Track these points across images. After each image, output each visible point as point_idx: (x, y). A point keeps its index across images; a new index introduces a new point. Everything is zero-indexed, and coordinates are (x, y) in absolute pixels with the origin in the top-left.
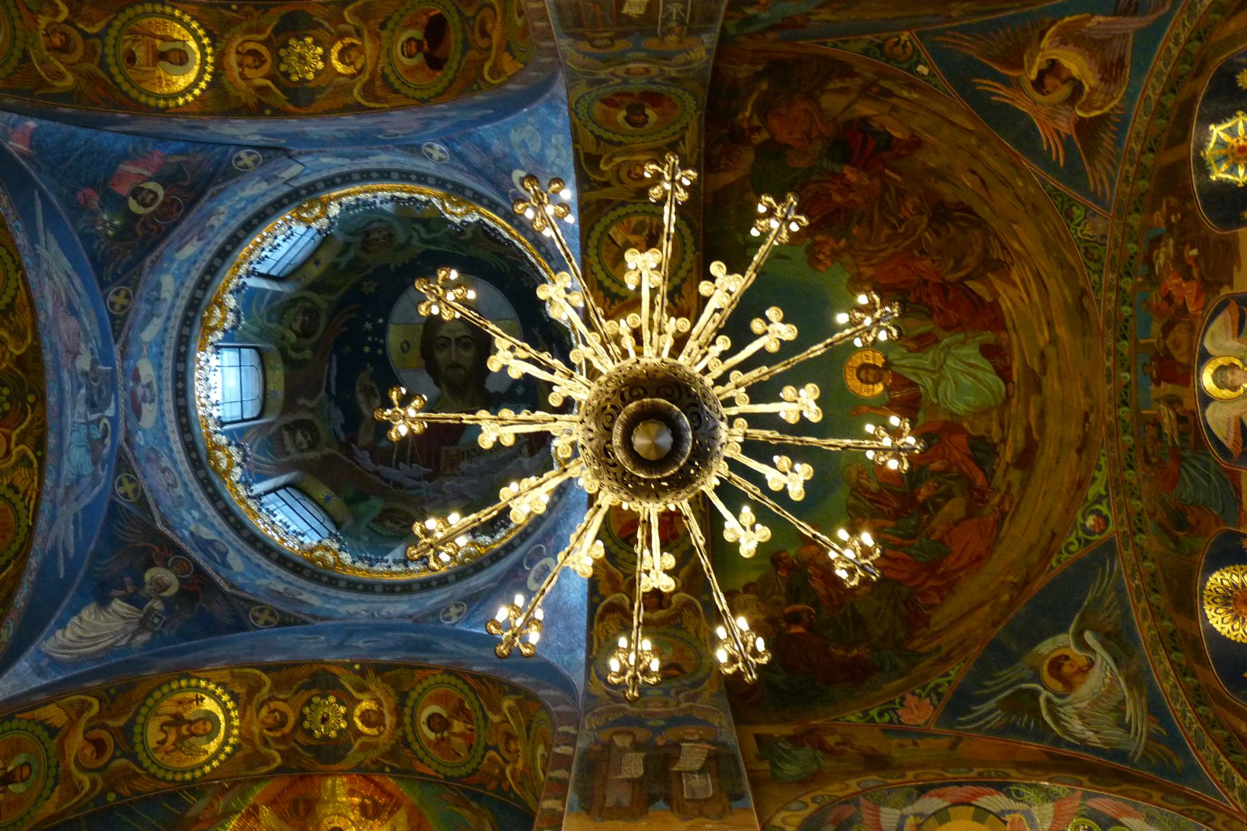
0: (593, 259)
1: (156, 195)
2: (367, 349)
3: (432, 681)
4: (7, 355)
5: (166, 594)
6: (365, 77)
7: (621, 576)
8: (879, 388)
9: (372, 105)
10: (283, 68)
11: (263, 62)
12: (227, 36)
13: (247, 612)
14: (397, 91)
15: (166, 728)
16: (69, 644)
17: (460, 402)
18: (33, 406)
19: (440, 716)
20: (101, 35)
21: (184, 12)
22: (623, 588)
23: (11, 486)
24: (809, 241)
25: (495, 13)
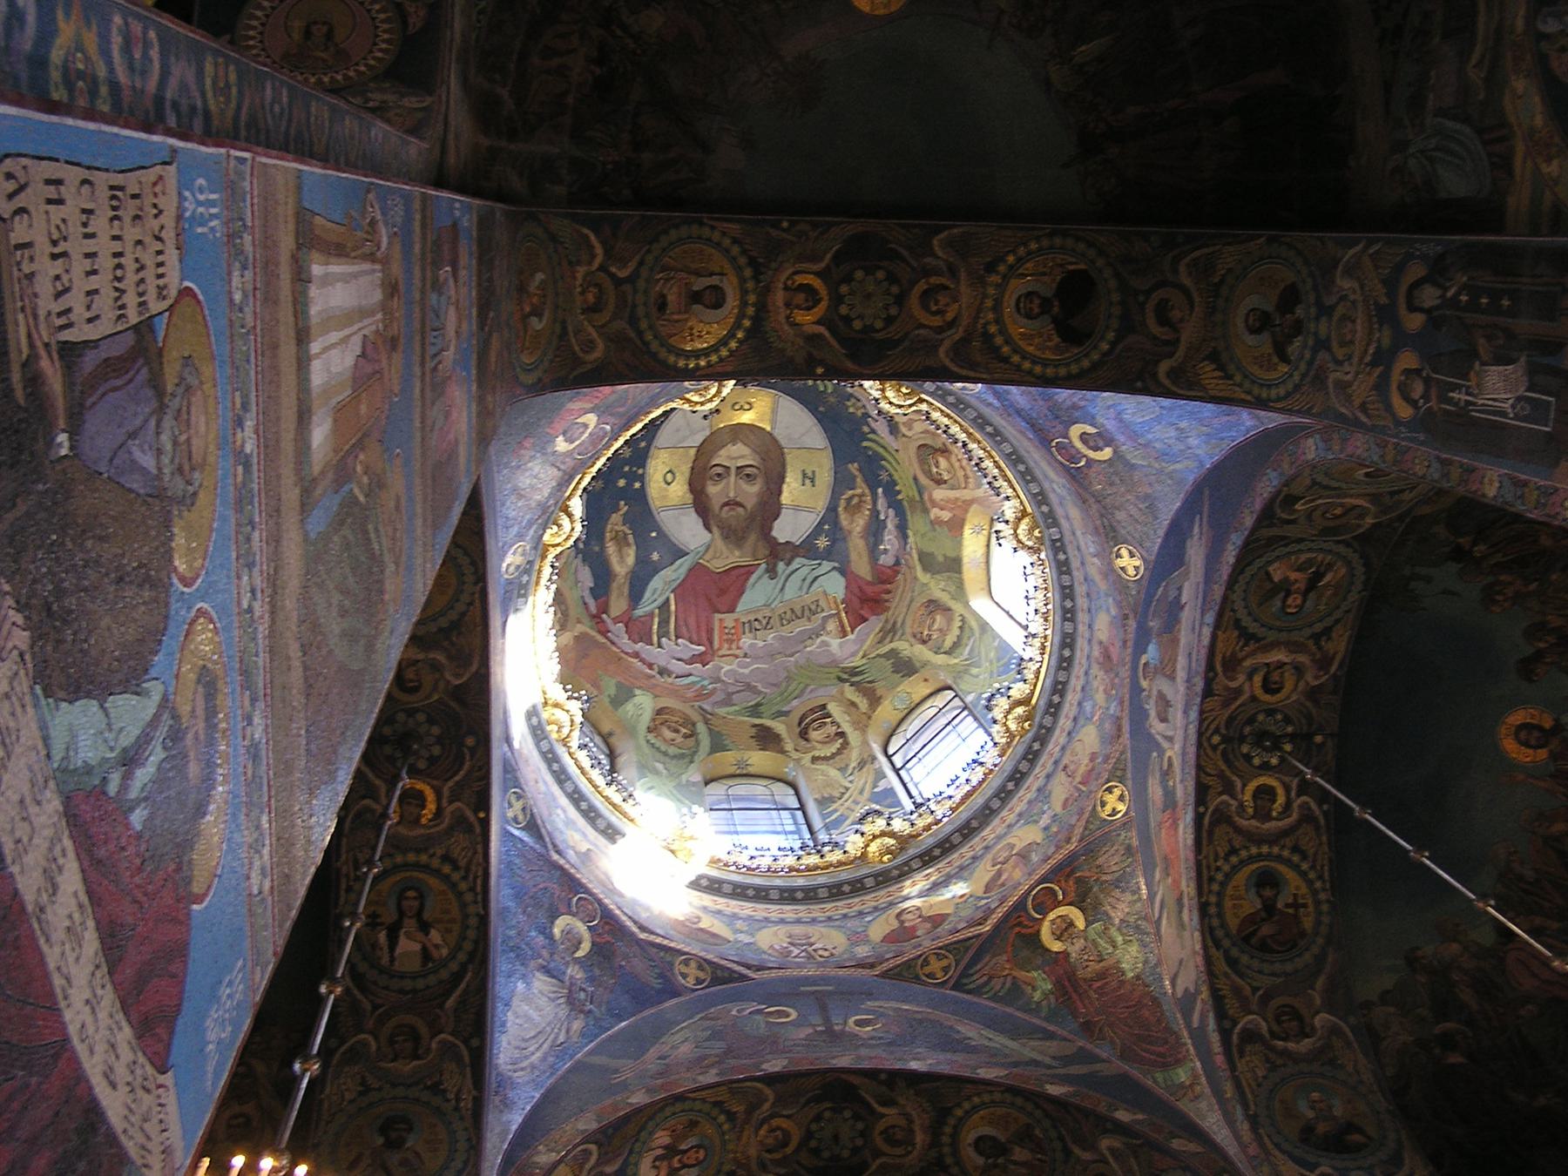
0: (1237, 596)
1: (586, 426)
2: (622, 483)
3: (986, 1098)
4: (442, 685)
5: (580, 954)
6: (957, 334)
7: (1248, 988)
8: (1542, 754)
9: (964, 372)
10: (844, 310)
11: (817, 302)
12: (773, 265)
13: (671, 964)
14: (1006, 360)
15: (657, 1163)
16: (517, 1054)
17: (737, 553)
18: (473, 751)
19: (993, 1139)
20: (632, 279)
21: (724, 234)
22: (1254, 1007)
23: (446, 858)
24: (1490, 579)
25: (1192, 307)
